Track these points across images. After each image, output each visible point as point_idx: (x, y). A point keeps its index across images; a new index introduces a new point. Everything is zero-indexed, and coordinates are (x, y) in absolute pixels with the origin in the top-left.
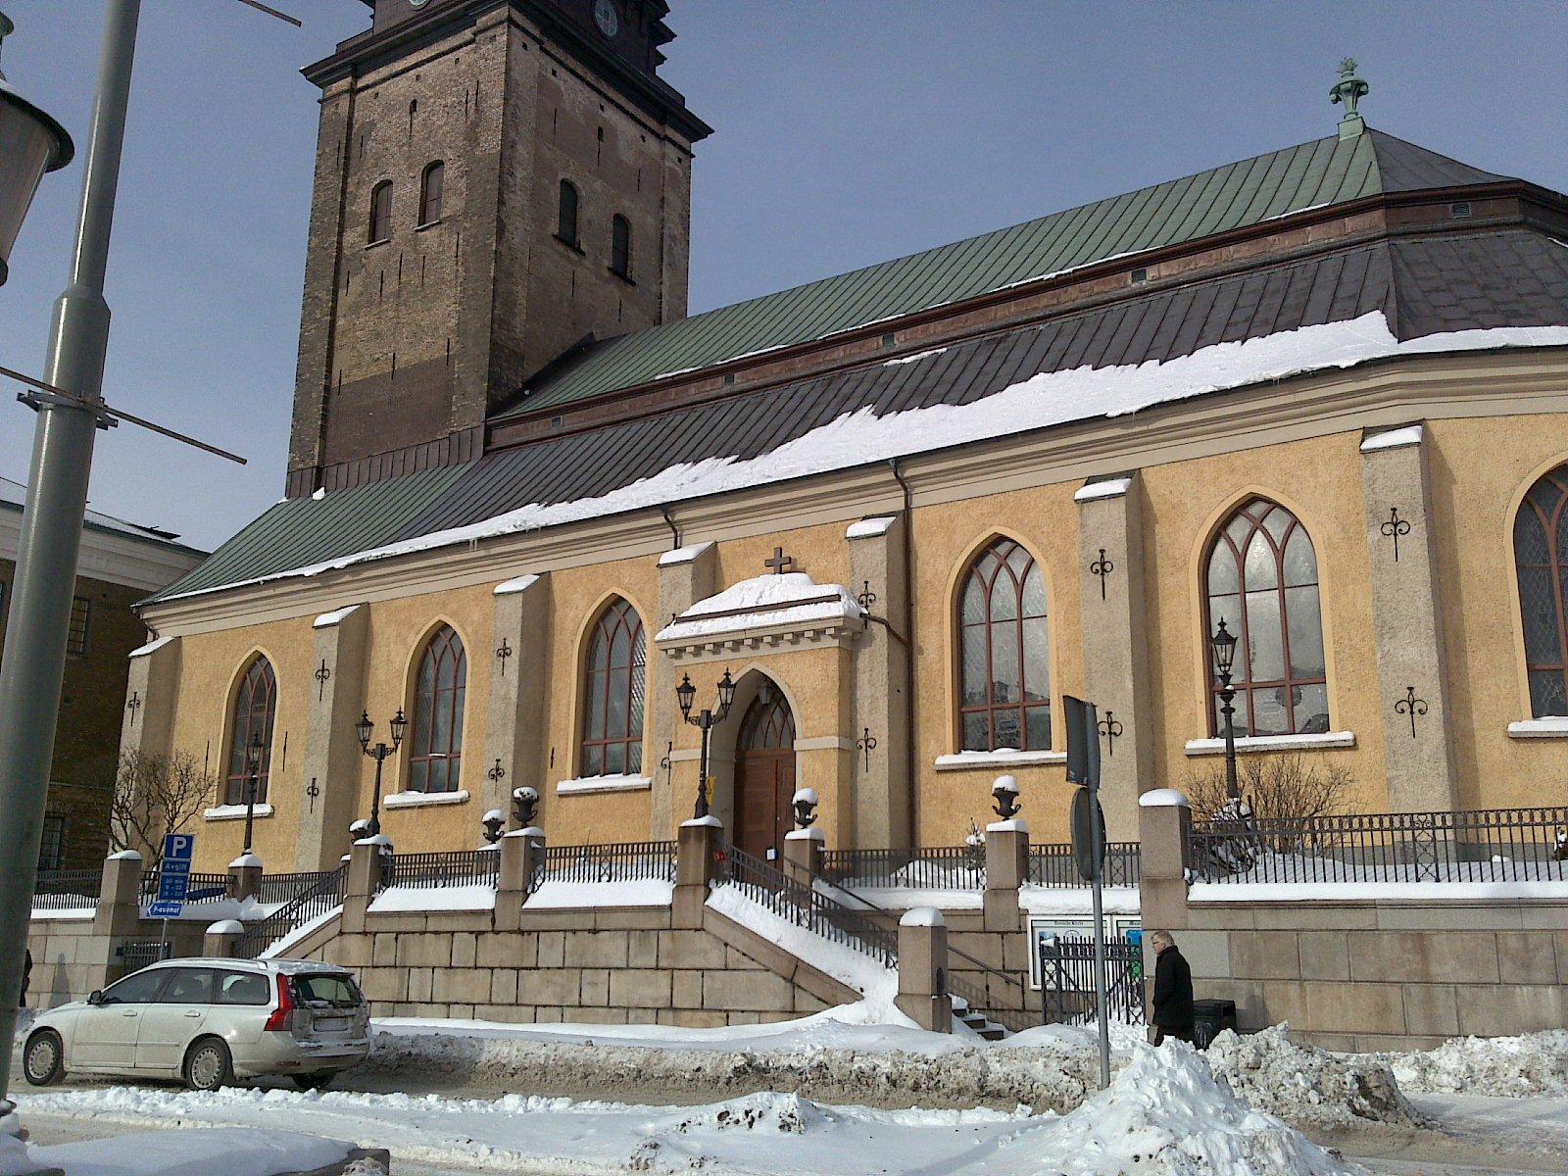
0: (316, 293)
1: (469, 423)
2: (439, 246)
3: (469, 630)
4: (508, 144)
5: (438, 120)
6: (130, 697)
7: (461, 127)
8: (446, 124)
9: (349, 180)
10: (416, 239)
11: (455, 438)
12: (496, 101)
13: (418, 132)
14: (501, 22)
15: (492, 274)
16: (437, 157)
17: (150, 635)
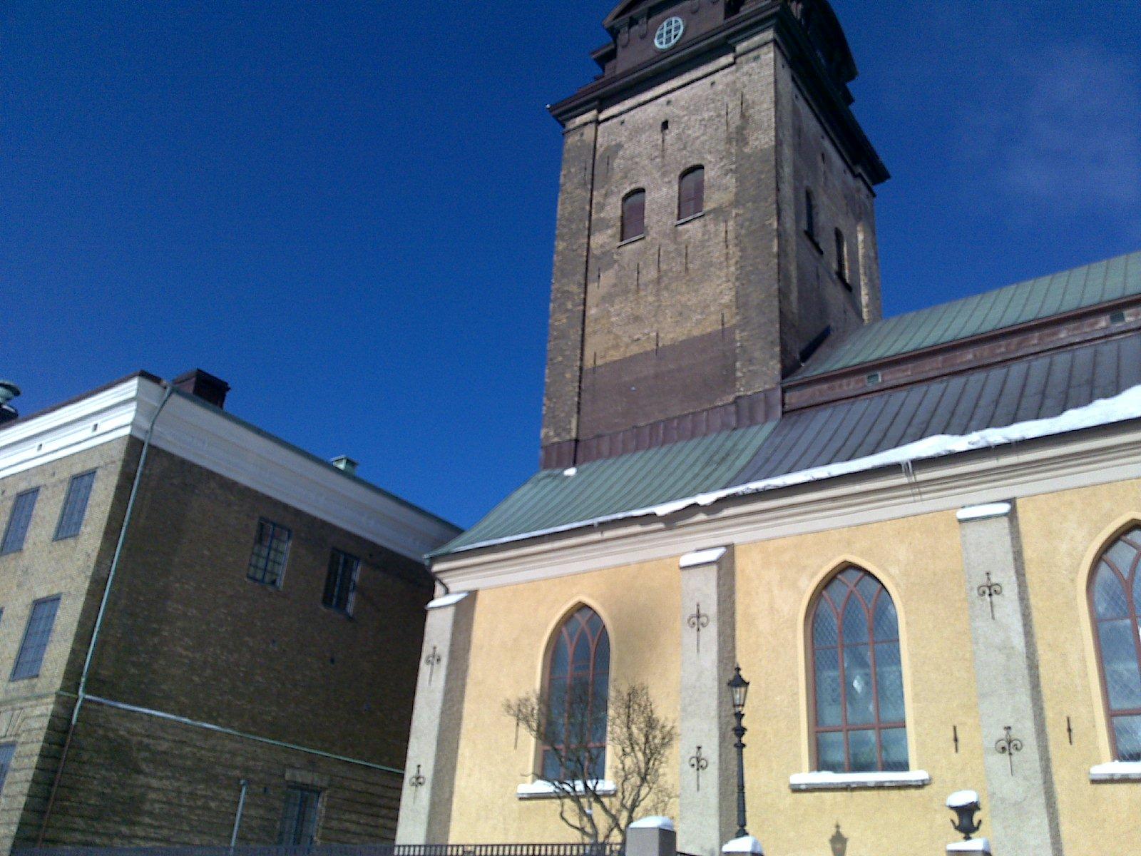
0: (566, 288)
1: (759, 386)
2: (703, 235)
3: (894, 570)
4: (779, 143)
6: (427, 650)
7: (722, 133)
8: (703, 134)
9: (595, 193)
10: (677, 231)
11: (744, 404)
12: (765, 106)
13: (671, 145)
14: (766, 44)
15: (775, 249)
16: (694, 161)
17: (439, 589)
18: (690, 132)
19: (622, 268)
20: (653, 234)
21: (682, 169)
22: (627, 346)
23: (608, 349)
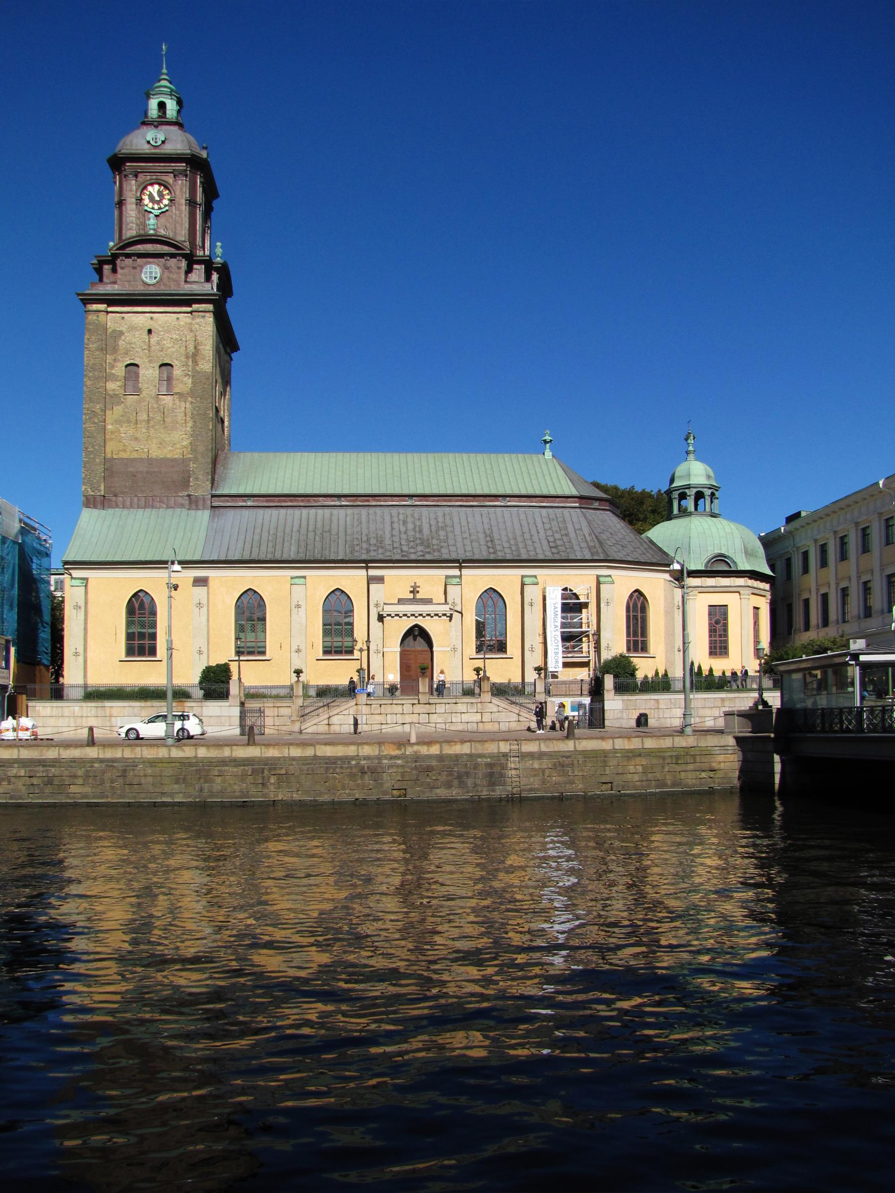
5: (167, 343)
18: (165, 342)
19: (126, 407)
20: (144, 394)
21: (161, 363)
22: (131, 452)
23: (120, 451)
